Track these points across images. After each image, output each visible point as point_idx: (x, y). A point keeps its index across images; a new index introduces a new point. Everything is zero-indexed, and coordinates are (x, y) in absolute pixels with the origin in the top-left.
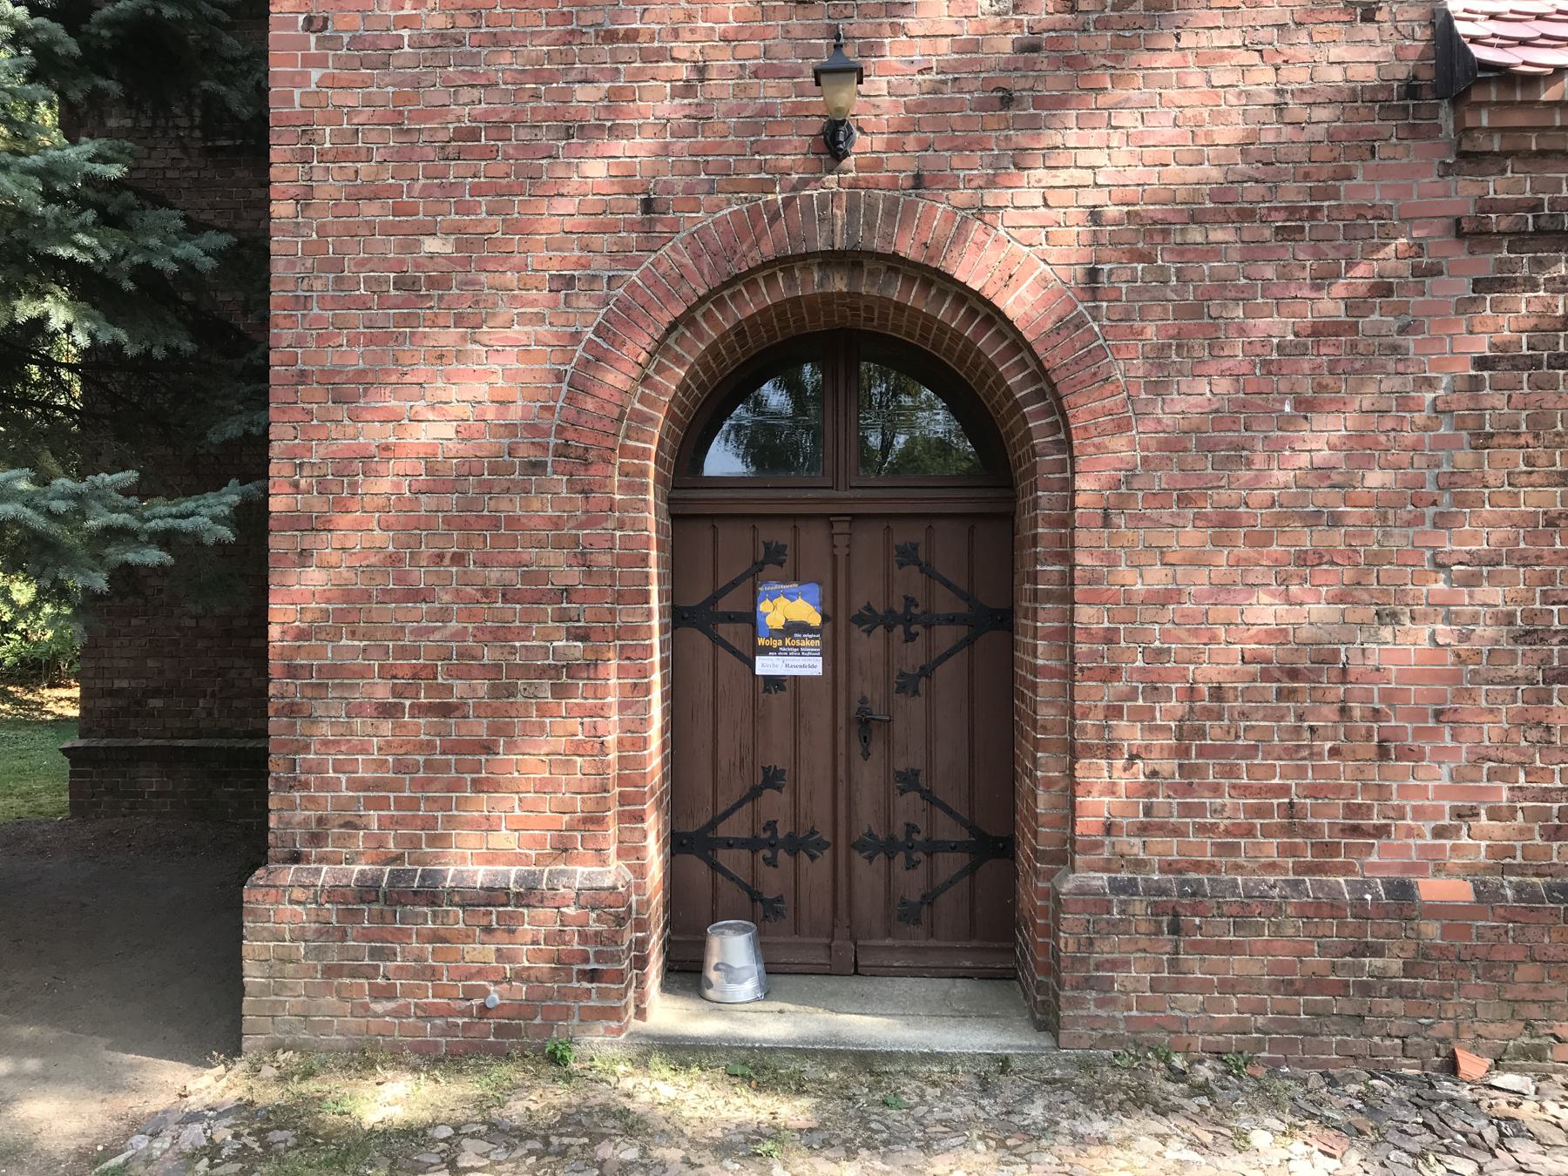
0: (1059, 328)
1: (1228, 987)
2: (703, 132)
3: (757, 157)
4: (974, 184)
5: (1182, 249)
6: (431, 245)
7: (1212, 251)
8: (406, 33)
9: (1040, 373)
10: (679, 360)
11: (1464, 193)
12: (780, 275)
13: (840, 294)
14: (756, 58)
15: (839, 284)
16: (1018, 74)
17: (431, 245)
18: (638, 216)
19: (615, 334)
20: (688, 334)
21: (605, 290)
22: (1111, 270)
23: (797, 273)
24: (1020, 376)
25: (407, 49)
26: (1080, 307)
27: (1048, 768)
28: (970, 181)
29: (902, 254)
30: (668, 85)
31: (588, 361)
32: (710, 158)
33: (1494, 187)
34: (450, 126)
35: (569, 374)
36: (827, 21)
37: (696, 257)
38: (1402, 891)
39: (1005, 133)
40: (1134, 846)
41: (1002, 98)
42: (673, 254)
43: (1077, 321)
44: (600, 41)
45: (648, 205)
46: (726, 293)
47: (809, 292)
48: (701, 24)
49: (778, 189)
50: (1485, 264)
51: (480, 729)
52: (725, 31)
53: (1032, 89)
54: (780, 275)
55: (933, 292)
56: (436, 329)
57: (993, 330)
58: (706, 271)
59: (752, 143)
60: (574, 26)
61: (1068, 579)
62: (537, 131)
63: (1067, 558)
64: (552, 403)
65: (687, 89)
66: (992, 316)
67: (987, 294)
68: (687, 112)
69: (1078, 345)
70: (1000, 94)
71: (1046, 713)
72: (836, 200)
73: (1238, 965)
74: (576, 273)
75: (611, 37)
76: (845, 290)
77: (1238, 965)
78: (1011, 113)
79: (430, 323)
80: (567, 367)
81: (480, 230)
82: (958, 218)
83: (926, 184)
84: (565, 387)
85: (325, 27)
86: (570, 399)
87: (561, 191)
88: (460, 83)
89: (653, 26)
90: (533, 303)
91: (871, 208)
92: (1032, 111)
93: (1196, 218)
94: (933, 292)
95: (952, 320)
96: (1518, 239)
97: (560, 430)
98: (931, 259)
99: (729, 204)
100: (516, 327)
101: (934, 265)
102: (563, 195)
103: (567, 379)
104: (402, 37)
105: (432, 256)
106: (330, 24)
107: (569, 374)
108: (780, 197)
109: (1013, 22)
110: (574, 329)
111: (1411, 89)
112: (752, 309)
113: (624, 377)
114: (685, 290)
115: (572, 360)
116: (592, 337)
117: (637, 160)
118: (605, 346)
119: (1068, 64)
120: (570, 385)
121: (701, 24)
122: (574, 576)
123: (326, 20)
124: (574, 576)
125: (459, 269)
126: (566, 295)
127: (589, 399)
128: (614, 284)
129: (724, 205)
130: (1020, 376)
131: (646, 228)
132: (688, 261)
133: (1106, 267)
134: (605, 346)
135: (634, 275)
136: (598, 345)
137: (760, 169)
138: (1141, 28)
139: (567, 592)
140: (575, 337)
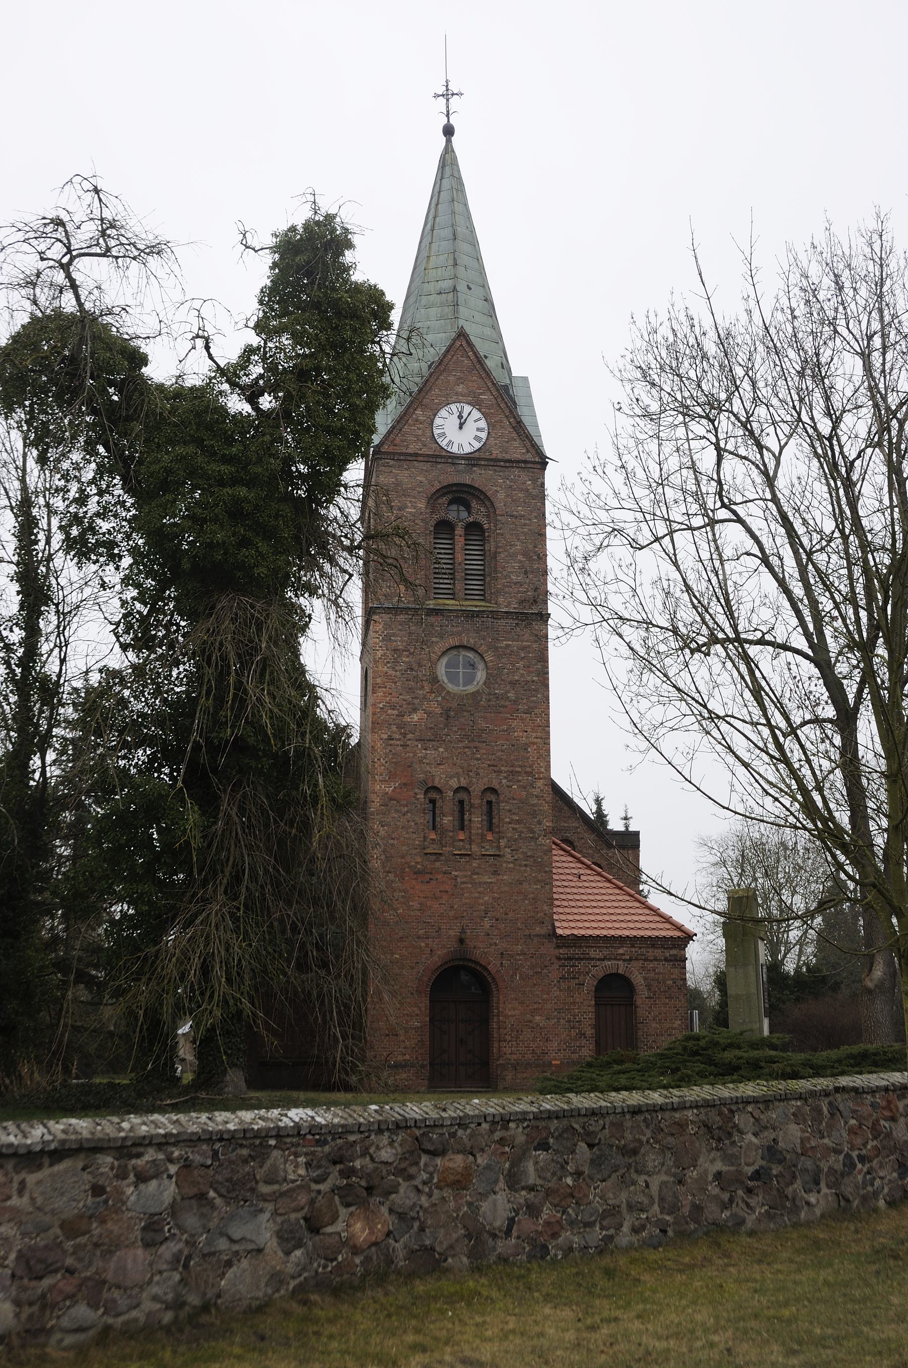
1: (524, 1079)
5: (515, 960)
7: (520, 960)
9: (494, 979)
11: (557, 952)
27: (496, 1045)
33: (561, 951)
38: (550, 1063)
40: (509, 1057)
42: (435, 958)
50: (561, 963)
51: (402, 1038)
61: (498, 1012)
63: (498, 1009)
66: (486, 969)
71: (495, 1035)
73: (525, 1075)
77: (525, 1075)
93: (518, 954)
96: (565, 959)
111: (549, 935)
122: (418, 1012)
124: (418, 1012)
131: (431, 954)
139: (417, 1015)
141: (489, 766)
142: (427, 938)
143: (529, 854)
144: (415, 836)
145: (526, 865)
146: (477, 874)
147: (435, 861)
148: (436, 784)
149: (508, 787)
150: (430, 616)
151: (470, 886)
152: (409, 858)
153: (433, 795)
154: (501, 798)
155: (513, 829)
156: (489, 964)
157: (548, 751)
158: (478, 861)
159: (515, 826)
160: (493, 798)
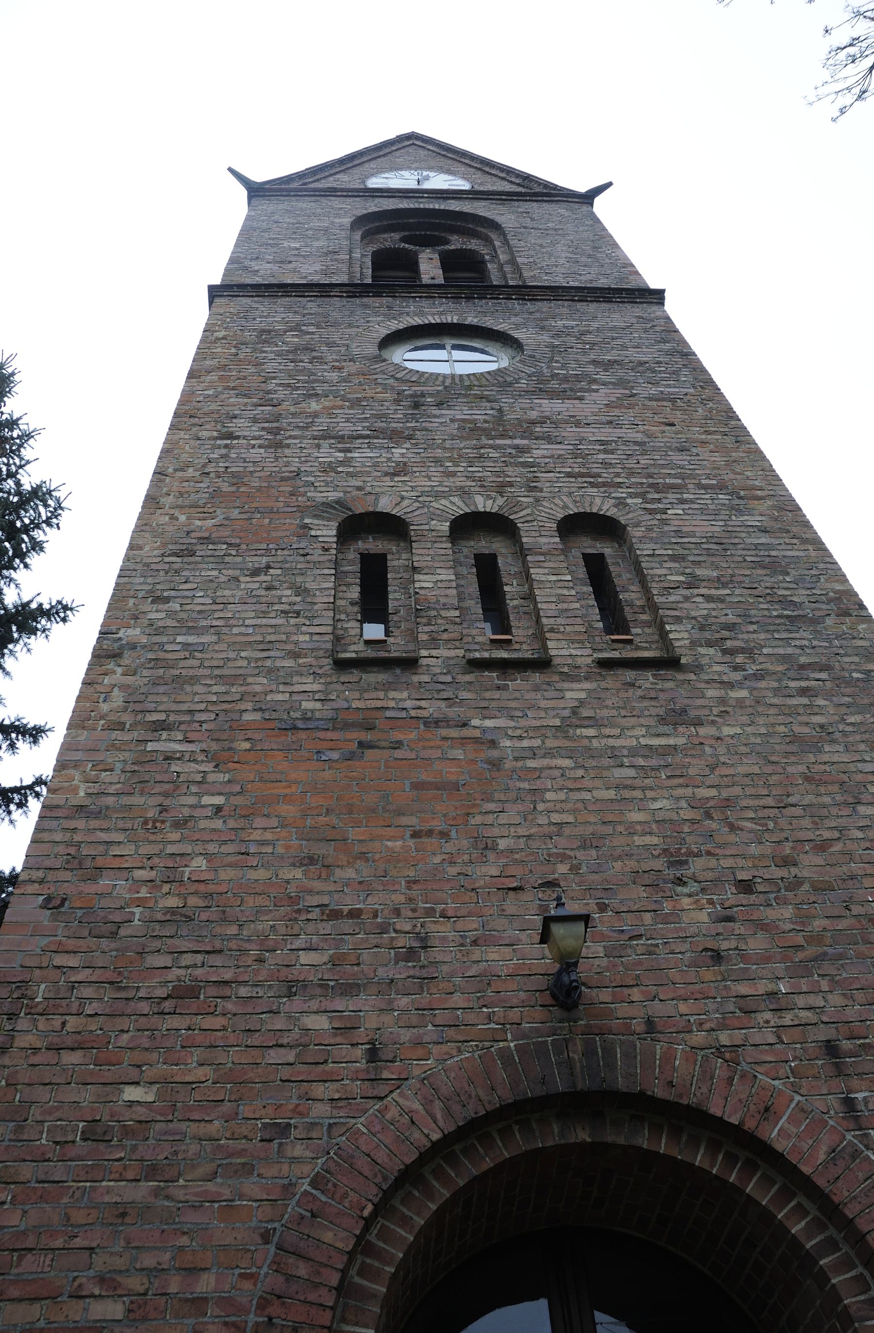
0: (833, 1158)
2: (428, 989)
3: (485, 1010)
4: (707, 1026)
6: (131, 1093)
8: (138, 911)
10: (405, 1222)
12: (516, 1128)
13: (583, 1144)
14: (476, 930)
15: (583, 1135)
16: (721, 937)
17: (131, 1093)
18: (362, 1065)
19: (335, 1185)
20: (417, 1194)
21: (325, 1138)
22: (865, 1098)
23: (535, 1126)
24: (803, 1223)
25: (136, 922)
26: (849, 1136)
28: (701, 1024)
29: (649, 1093)
30: (392, 951)
31: (302, 1217)
32: (437, 1012)
34: (169, 984)
35: (278, 1234)
36: (538, 902)
37: (427, 1103)
39: (723, 983)
41: (712, 957)
43: (849, 1150)
44: (325, 918)
45: (373, 1055)
46: (457, 1148)
47: (550, 1143)
48: (421, 905)
49: (509, 1036)
52: (444, 910)
53: (736, 949)
54: (516, 1128)
55: (684, 1138)
56: (123, 1183)
57: (758, 1175)
58: (439, 1116)
59: (478, 998)
60: (301, 906)
62: (258, 989)
64: (254, 1270)
65: (410, 954)
67: (750, 1125)
68: (411, 973)
69: (861, 1175)
70: (710, 953)
72: (570, 1045)
74: (292, 1121)
75: (335, 915)
76: (589, 1140)
78: (723, 968)
79: (117, 1176)
80: (276, 1225)
81: (188, 1079)
82: (699, 1058)
83: (659, 1029)
84: (272, 1248)
85: (62, 905)
86: (277, 1267)
87: (280, 1042)
88: (185, 949)
89: (376, 906)
90: (241, 1153)
91: (609, 1051)
92: (742, 965)
94: (684, 1138)
95: (712, 1167)
97: (263, 1304)
98: (681, 1096)
99: (459, 1051)
100: (219, 1180)
101: (685, 1101)
102: (281, 1046)
103: (275, 1239)
104: (133, 914)
105: (131, 1104)
106: (67, 904)
107: (278, 1234)
108: (512, 1045)
109: (705, 901)
110: (286, 1182)
112: (488, 1163)
113: (345, 1234)
114: (417, 1135)
115: (283, 1216)
116: (308, 1188)
117: (362, 1014)
118: (324, 1199)
119: (762, 929)
120: (279, 1247)
121: (421, 905)
123: (64, 900)
125: (159, 1118)
126: (280, 1144)
127: (301, 1264)
128: (335, 1132)
129: (454, 1052)
130: (803, 1223)
132: (417, 1106)
133: (860, 1096)
134: (324, 1199)
135: (360, 1124)
136: (315, 1197)
137: (489, 1018)
138: (814, 902)
140: (288, 1188)
141: (569, 475)
142: (349, 989)
143: (803, 660)
144: (293, 621)
145: (803, 692)
146: (594, 722)
147: (387, 687)
148: (385, 505)
149: (651, 512)
150: (360, 296)
151: (567, 763)
152: (260, 683)
153: (372, 545)
154: (635, 533)
155: (709, 598)
156: (768, 1112)
157: (759, 452)
158: (587, 685)
159: (713, 592)
160: (607, 550)
